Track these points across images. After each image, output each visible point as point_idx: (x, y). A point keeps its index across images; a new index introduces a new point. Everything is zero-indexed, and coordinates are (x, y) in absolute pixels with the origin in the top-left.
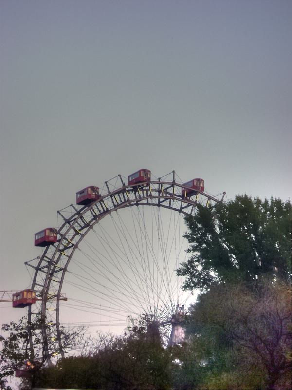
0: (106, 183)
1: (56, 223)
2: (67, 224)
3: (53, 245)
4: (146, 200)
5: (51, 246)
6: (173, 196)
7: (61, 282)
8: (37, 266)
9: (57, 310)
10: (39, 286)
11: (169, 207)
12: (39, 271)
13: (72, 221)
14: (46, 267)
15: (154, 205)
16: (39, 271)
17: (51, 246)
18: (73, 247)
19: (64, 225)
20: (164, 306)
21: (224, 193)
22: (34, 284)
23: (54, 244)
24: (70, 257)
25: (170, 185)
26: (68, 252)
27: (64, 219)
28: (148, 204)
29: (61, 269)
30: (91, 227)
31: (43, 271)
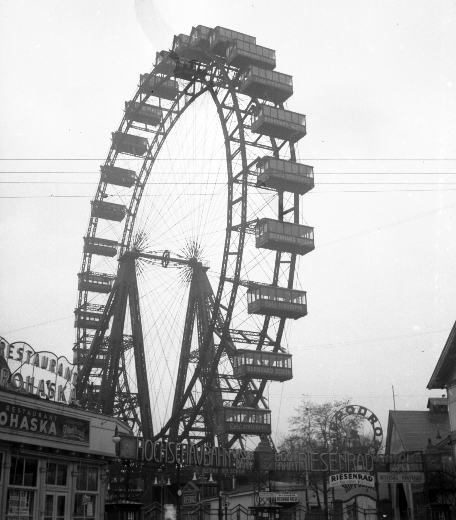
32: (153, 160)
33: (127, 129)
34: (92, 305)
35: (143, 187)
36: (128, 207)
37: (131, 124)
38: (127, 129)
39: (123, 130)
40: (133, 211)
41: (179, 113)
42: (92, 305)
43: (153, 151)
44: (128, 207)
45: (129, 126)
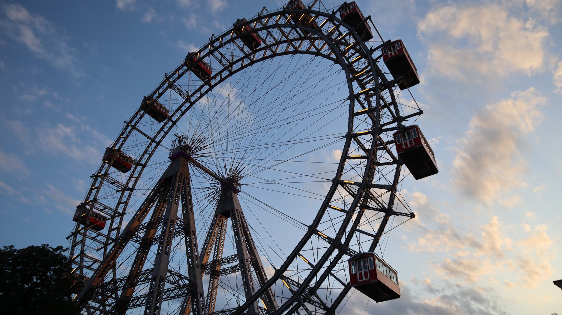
21: (67, 238)
32: (211, 88)
33: (207, 54)
34: (110, 178)
35: (192, 104)
36: (170, 114)
37: (213, 52)
38: (207, 54)
39: (202, 54)
40: (174, 119)
41: (253, 62)
42: (110, 178)
43: (213, 82)
44: (170, 114)
45: (211, 53)
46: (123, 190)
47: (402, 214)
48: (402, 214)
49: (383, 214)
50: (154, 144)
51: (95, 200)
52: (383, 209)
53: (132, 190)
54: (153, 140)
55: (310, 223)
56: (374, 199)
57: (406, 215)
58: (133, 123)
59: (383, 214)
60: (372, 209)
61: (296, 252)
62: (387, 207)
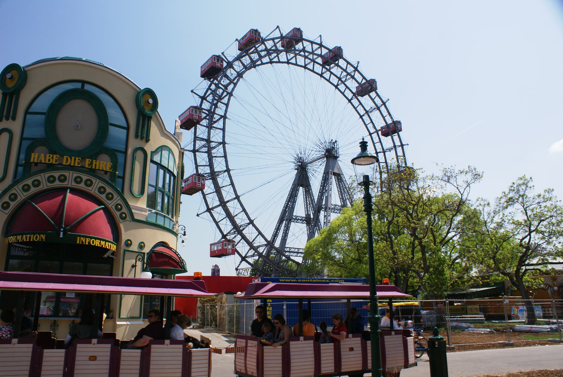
0: (223, 53)
1: (196, 102)
2: (204, 101)
3: (199, 124)
4: (260, 61)
5: (198, 125)
6: (278, 52)
7: (225, 156)
8: (192, 149)
9: (232, 184)
10: (203, 167)
11: (279, 62)
12: (197, 153)
13: (209, 95)
14: (204, 146)
15: (267, 63)
16: (197, 153)
17: (198, 125)
18: (223, 119)
19: (202, 102)
20: (312, 145)
21: (320, 36)
22: (197, 167)
23: (201, 123)
24: (223, 130)
25: (279, 39)
26: (220, 124)
27: (200, 97)
28: (262, 64)
29: (220, 143)
30: (230, 94)
31: (200, 152)
46: (340, 79)
47: (240, 264)
48: (240, 264)
49: (244, 255)
50: (362, 112)
51: (338, 65)
52: (246, 257)
53: (336, 87)
54: (367, 112)
55: (255, 222)
56: (253, 256)
57: (238, 267)
58: (383, 109)
59: (244, 255)
60: (249, 251)
61: (244, 210)
62: (246, 259)
